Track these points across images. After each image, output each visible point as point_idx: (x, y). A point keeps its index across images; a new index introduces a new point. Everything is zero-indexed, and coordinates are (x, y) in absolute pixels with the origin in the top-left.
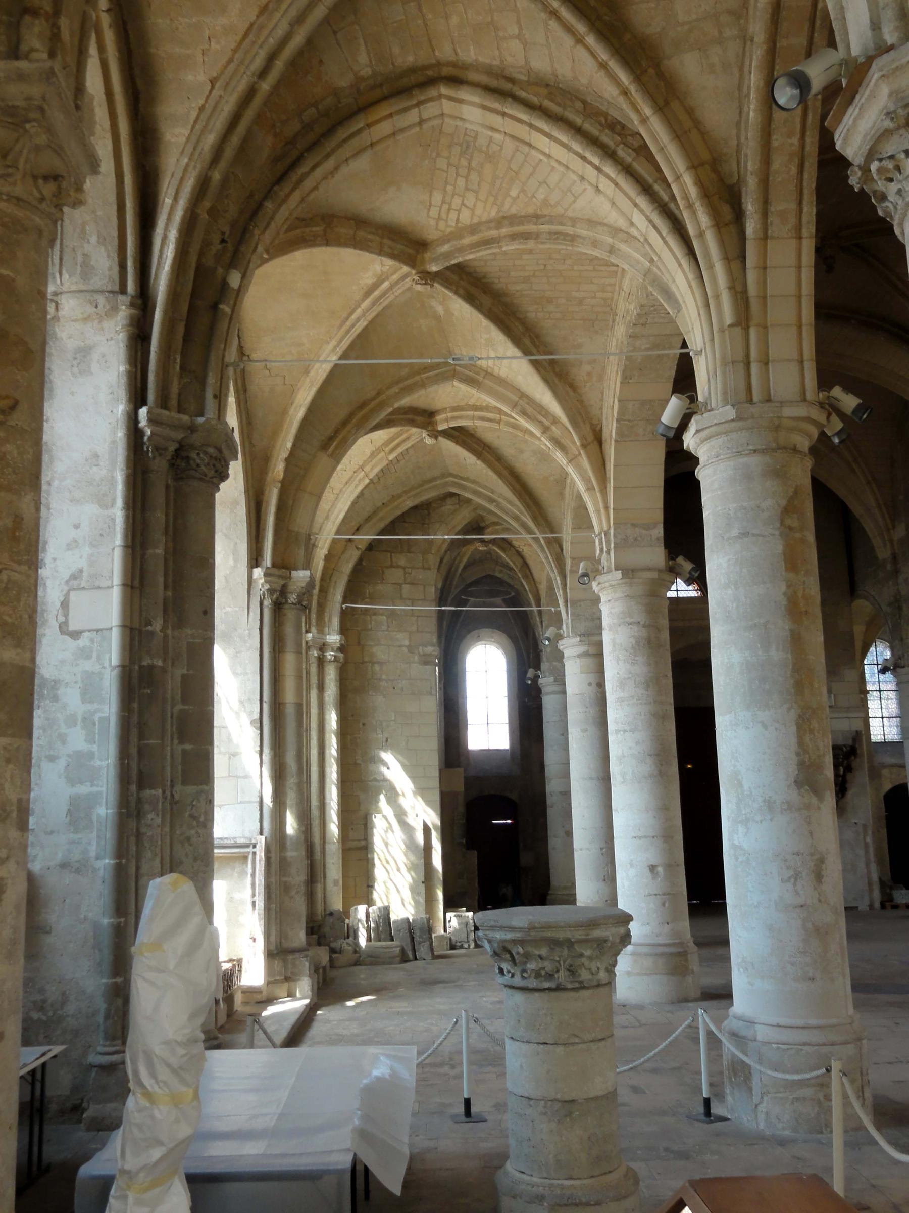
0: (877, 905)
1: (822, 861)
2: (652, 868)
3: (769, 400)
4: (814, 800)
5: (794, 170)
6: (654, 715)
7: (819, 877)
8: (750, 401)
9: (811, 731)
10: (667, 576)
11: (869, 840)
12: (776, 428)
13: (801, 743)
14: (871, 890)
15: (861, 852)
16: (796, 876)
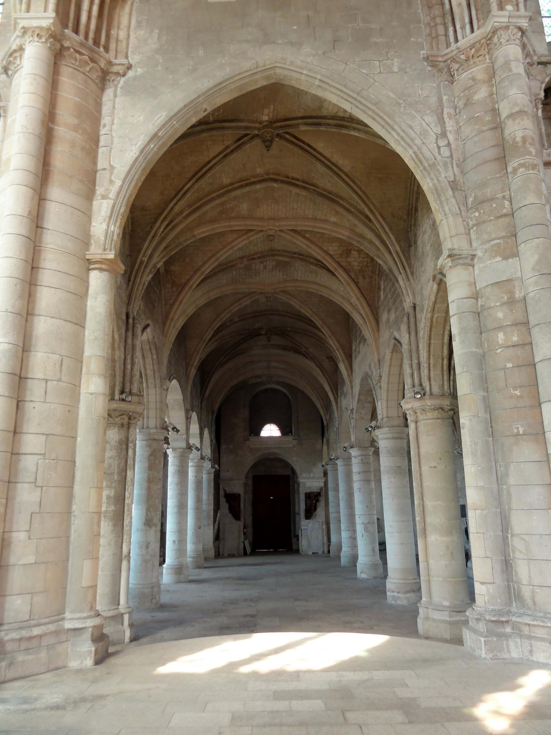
0: (326, 551)
1: (149, 543)
2: (174, 542)
3: (148, 428)
4: (149, 528)
5: (152, 373)
6: (179, 494)
7: (147, 547)
8: (143, 428)
9: (150, 511)
10: (188, 450)
11: (324, 527)
12: (149, 434)
13: (147, 514)
14: (323, 546)
15: (320, 532)
16: (142, 547)
